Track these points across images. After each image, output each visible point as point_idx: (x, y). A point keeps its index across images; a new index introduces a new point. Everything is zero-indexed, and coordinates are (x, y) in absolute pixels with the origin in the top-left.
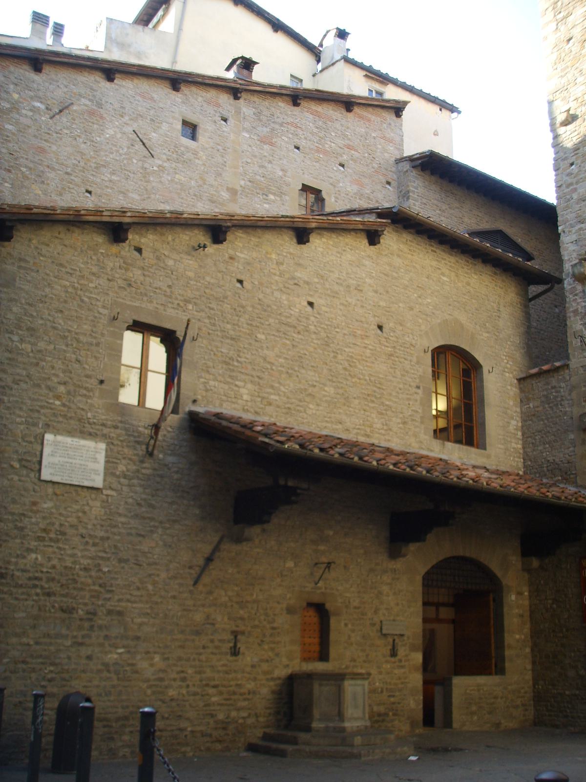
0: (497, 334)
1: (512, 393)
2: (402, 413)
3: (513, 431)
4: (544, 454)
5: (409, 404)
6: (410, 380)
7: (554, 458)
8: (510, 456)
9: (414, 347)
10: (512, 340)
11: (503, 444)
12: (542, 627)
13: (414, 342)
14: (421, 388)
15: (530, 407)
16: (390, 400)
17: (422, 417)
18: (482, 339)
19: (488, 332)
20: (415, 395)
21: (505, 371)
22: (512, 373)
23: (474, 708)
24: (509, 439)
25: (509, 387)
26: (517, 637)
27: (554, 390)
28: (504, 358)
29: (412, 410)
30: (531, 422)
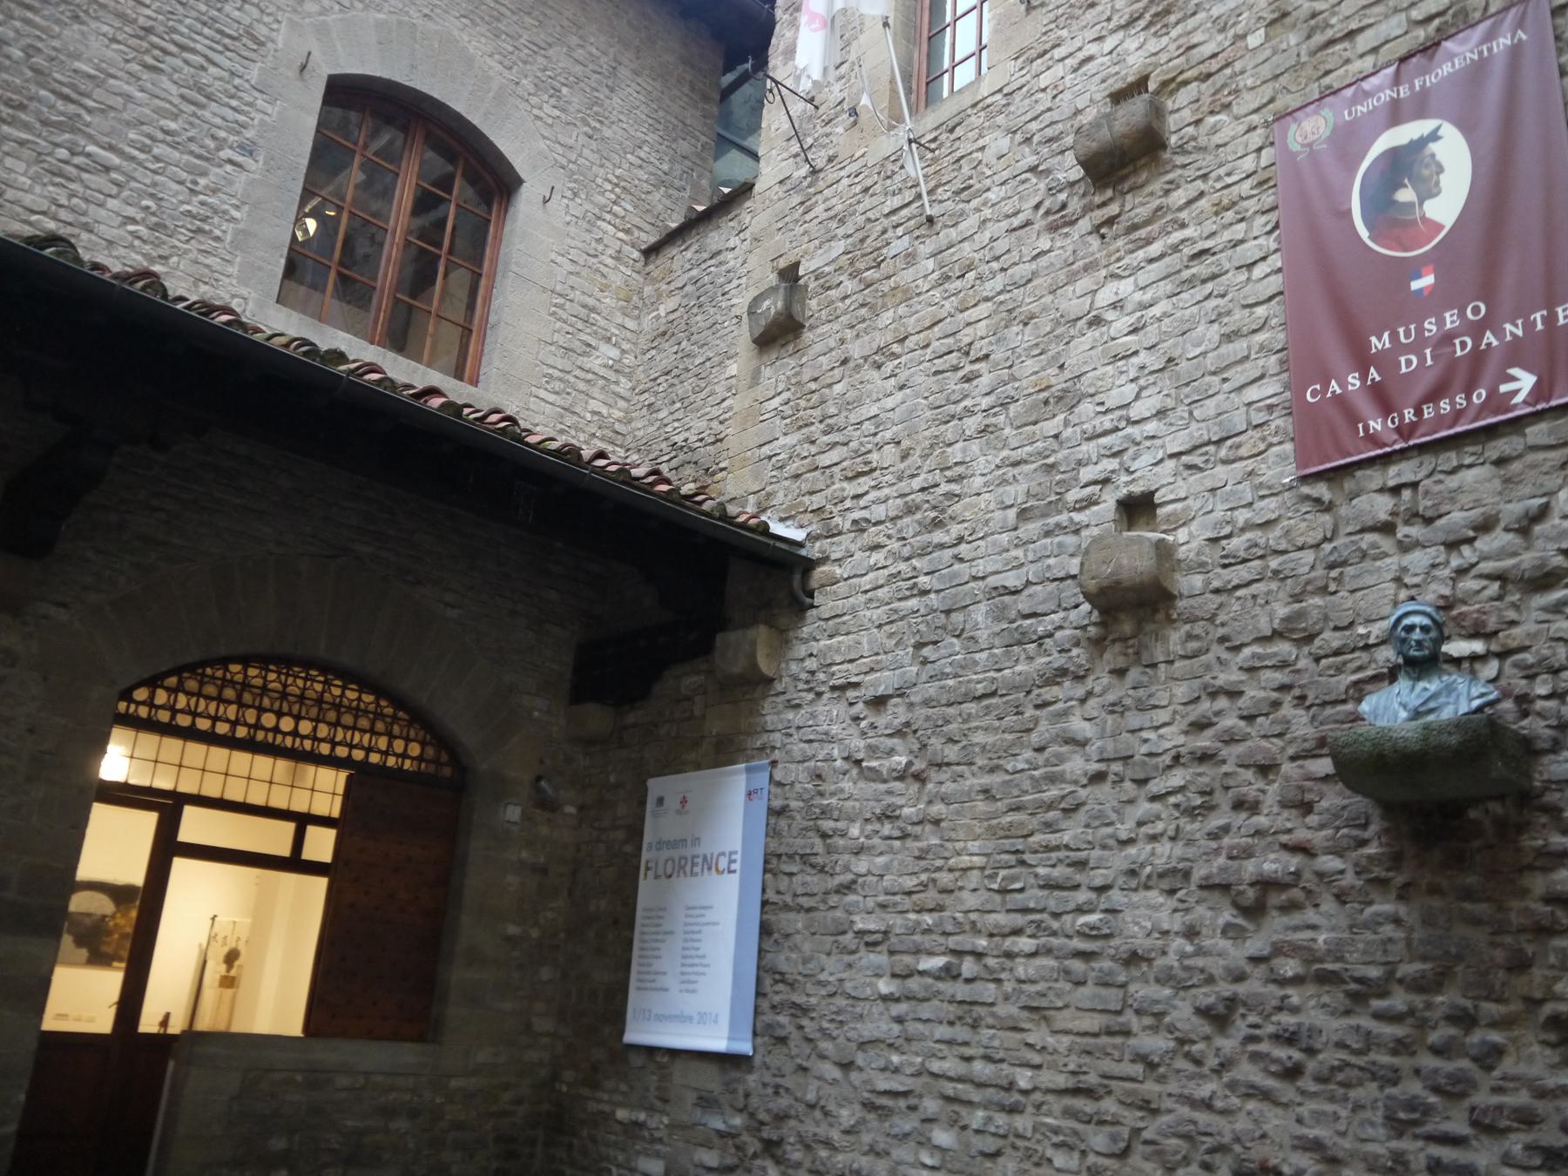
0: (594, 124)
1: (616, 280)
2: (152, 196)
3: (602, 372)
4: (669, 429)
5: (195, 183)
6: (218, 121)
7: (686, 435)
8: (578, 429)
9: (262, 44)
10: (642, 155)
11: (557, 393)
12: (592, 908)
13: (262, 31)
14: (261, 159)
15: (658, 317)
16: (111, 148)
17: (238, 232)
18: (537, 118)
19: (563, 110)
20: (229, 168)
21: (599, 218)
22: (627, 232)
23: (278, 1144)
24: (581, 386)
25: (609, 261)
26: (512, 930)
27: (713, 262)
28: (609, 187)
29: (203, 203)
30: (653, 352)
